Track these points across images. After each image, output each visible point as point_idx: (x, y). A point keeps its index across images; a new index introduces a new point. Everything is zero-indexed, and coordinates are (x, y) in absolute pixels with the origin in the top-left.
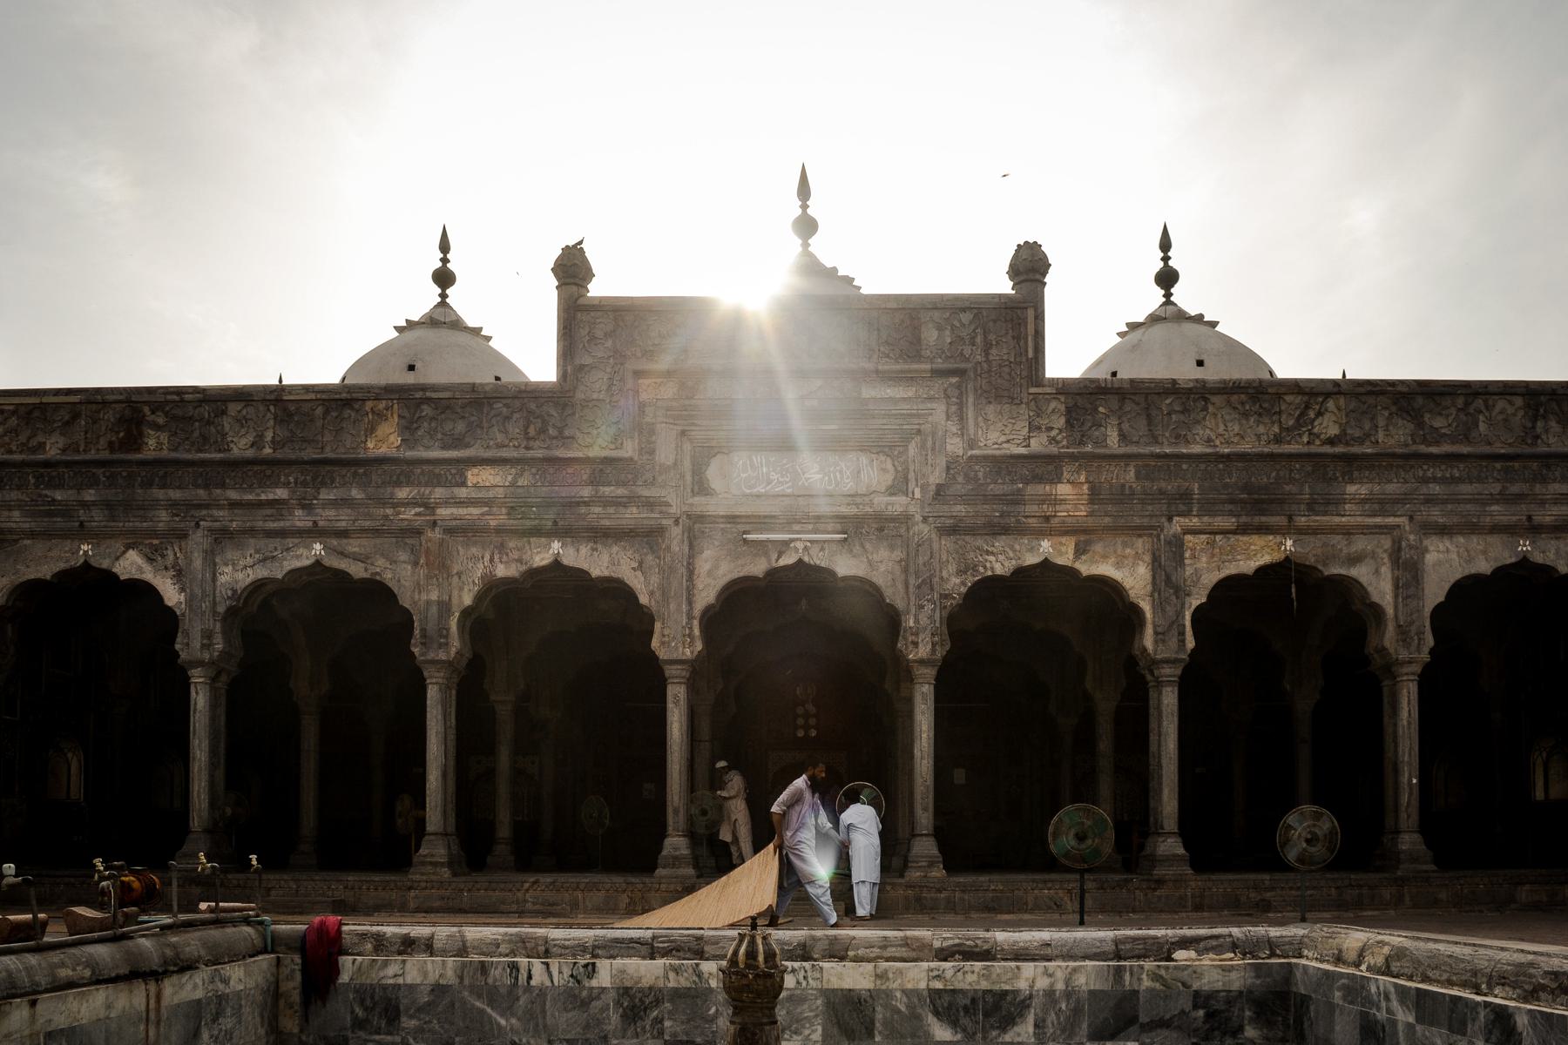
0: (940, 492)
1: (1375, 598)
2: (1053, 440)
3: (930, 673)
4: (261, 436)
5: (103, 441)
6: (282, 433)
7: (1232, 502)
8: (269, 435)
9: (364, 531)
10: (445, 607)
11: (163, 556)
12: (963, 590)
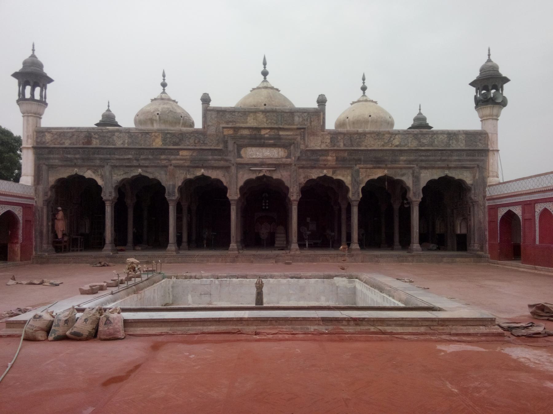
0: (299, 159)
1: (408, 185)
2: (327, 146)
4: (124, 141)
5: (81, 142)
6: (130, 140)
7: (372, 161)
8: (126, 141)
9: (152, 166)
10: (174, 186)
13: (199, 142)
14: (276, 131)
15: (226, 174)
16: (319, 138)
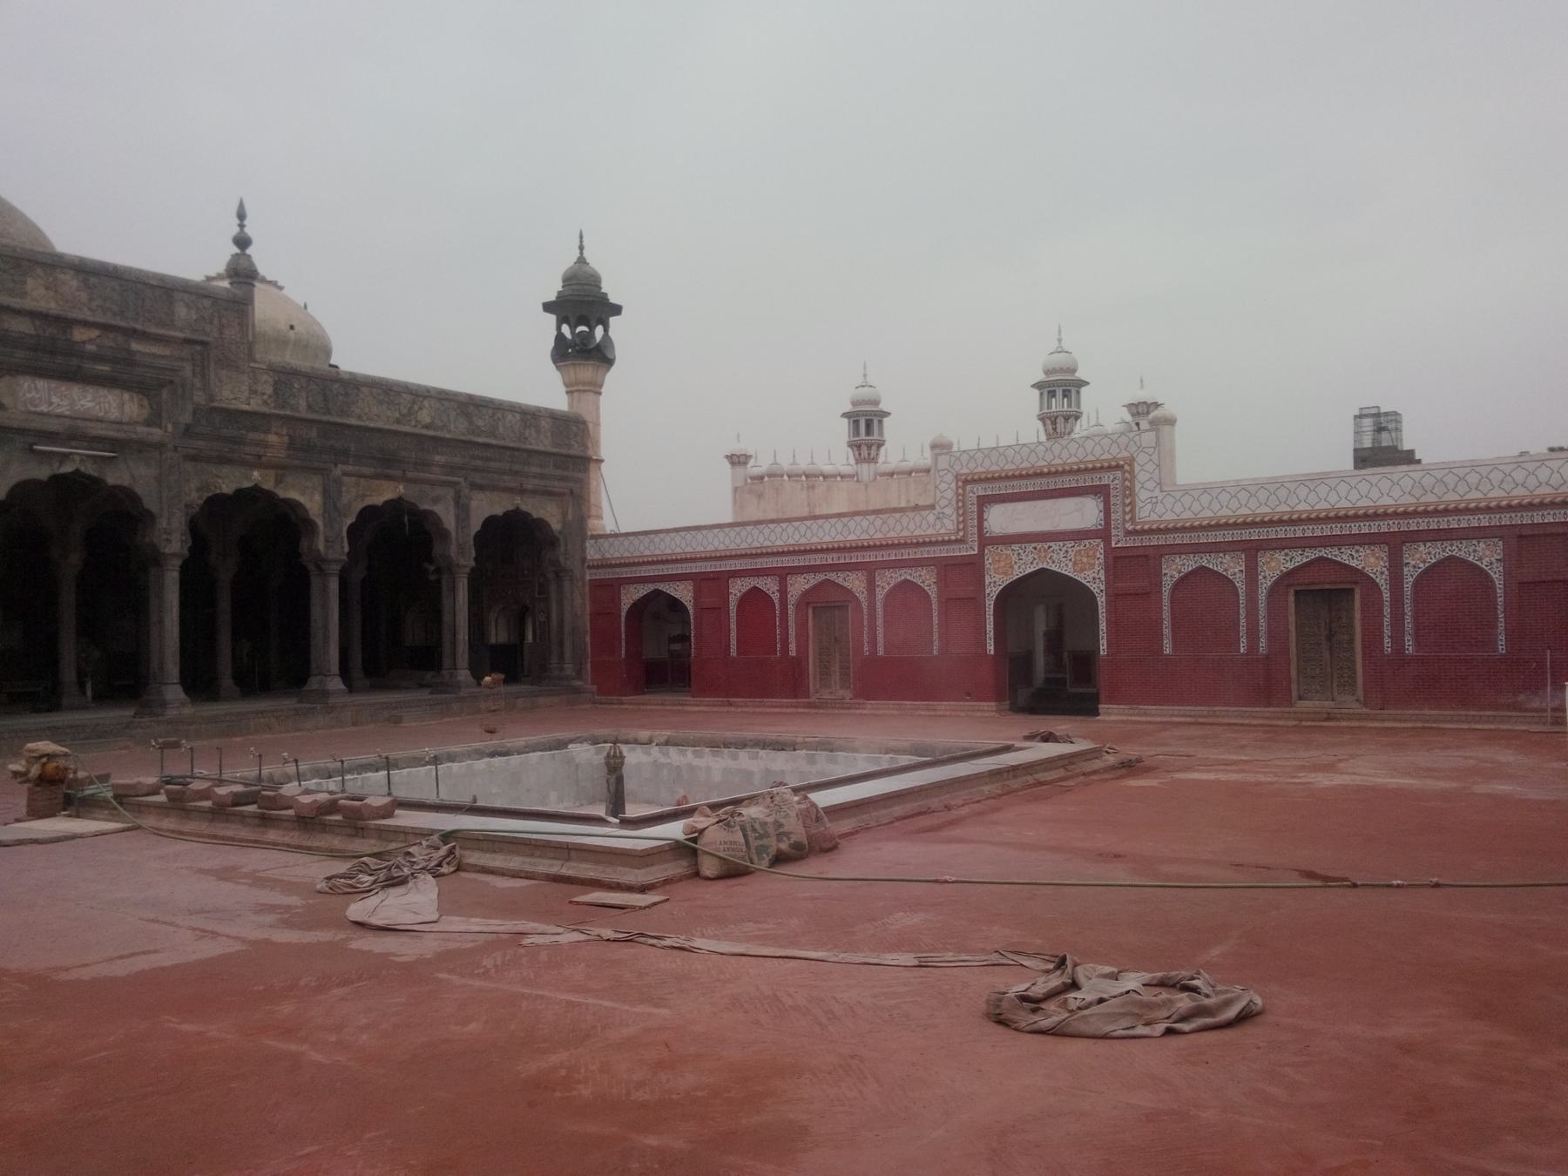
0: (188, 432)
1: (446, 525)
2: (265, 402)
3: (178, 562)
14: (120, 338)
16: (245, 378)
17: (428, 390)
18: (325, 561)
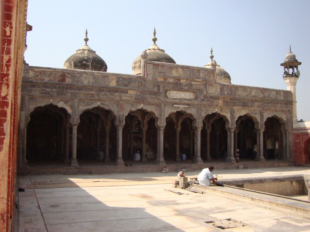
4: (89, 81)
6: (94, 81)
8: (91, 81)
11: (68, 103)
12: (205, 116)
13: (141, 84)
15: (158, 108)
17: (254, 87)
18: (231, 129)
